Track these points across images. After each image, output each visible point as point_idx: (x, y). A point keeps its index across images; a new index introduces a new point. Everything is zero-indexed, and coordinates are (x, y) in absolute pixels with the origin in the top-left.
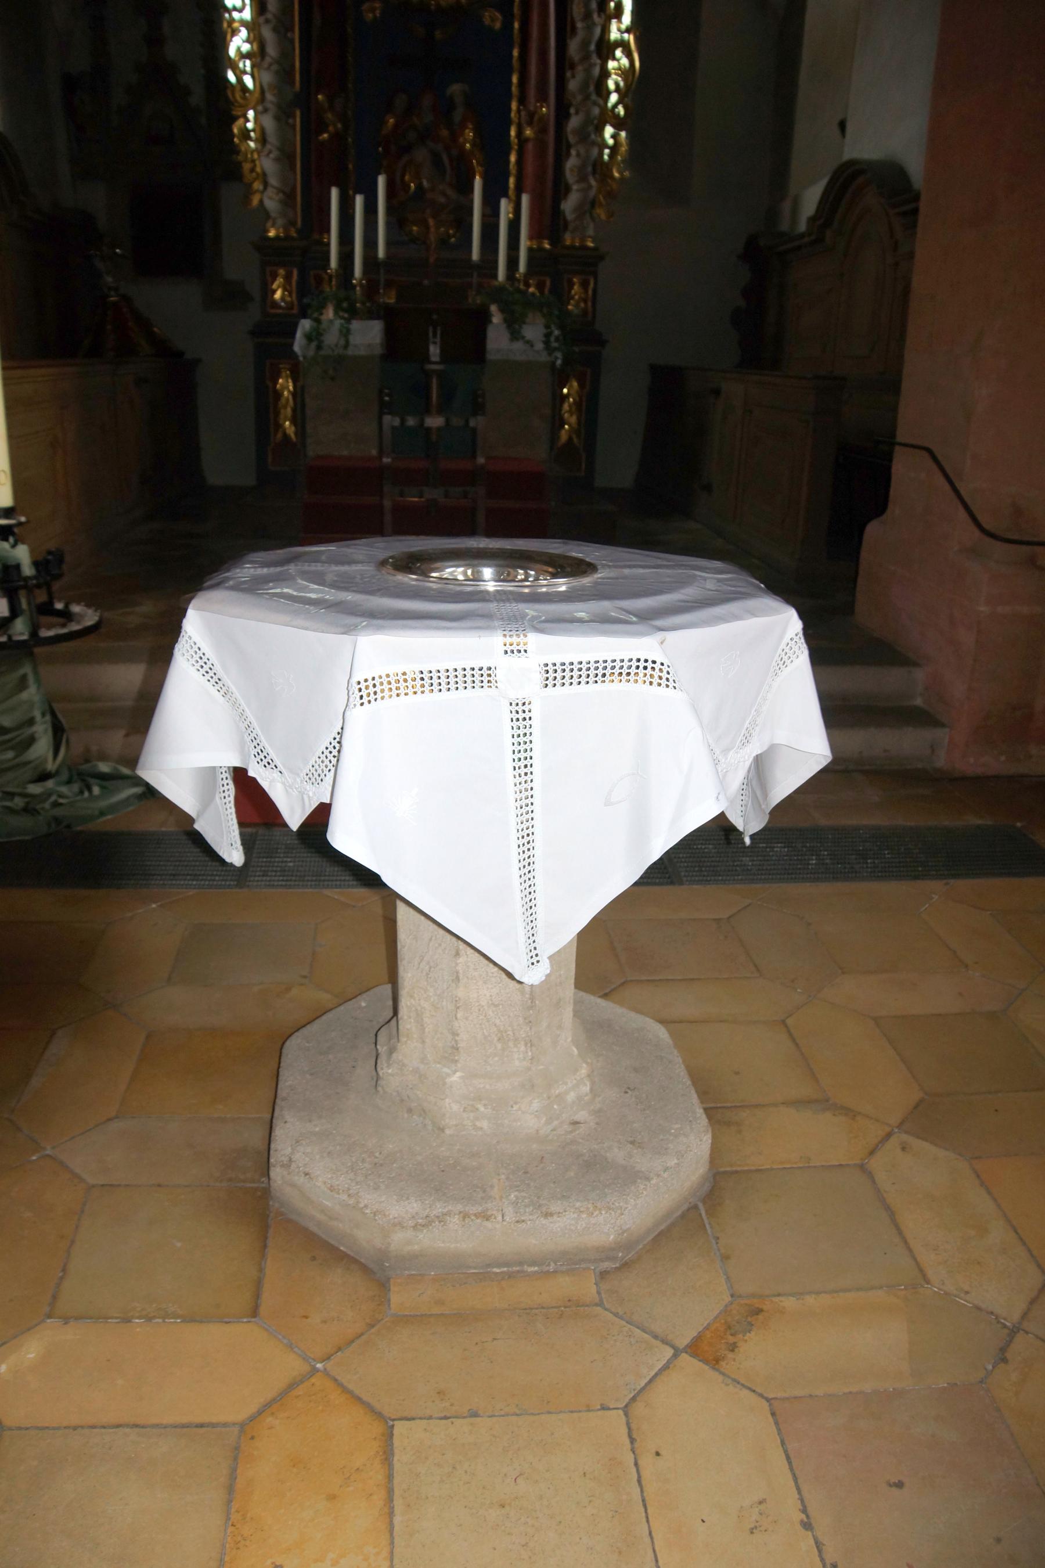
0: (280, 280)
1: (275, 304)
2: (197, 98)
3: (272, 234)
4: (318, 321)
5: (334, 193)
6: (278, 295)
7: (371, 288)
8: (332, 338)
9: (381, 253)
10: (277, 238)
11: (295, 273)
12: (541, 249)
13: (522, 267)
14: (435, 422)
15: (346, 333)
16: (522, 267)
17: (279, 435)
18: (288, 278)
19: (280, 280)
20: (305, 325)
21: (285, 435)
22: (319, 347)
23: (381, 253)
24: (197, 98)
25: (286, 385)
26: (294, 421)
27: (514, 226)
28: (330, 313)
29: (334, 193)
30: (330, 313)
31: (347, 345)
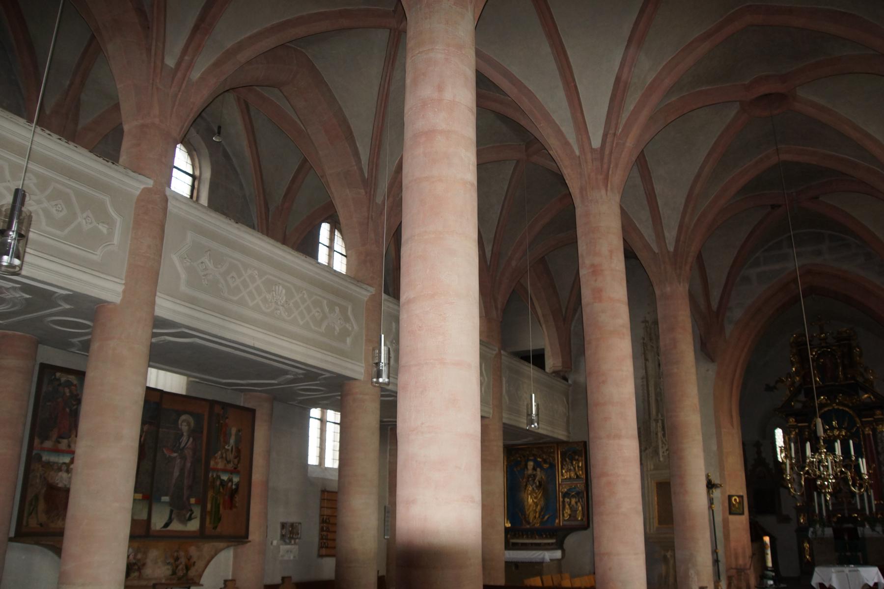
0: (802, 517)
1: (801, 523)
2: (771, 466)
3: (799, 504)
4: (815, 528)
5: (815, 493)
6: (802, 521)
7: (828, 515)
8: (819, 532)
9: (831, 508)
10: (800, 505)
11: (806, 515)
12: (881, 503)
13: (874, 510)
14: (848, 554)
15: (823, 531)
16: (874, 510)
17: (806, 560)
18: (804, 516)
19: (802, 517)
20: (811, 529)
21: (808, 559)
22: (816, 535)
23: (831, 508)
24: (771, 466)
25: (807, 545)
26: (809, 556)
27: (869, 497)
28: (818, 526)
29: (815, 493)
30: (818, 526)
31: (824, 534)
